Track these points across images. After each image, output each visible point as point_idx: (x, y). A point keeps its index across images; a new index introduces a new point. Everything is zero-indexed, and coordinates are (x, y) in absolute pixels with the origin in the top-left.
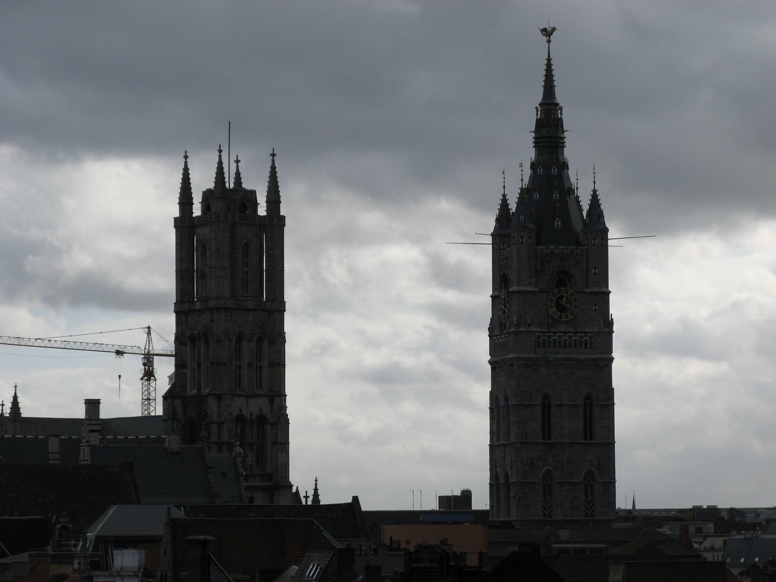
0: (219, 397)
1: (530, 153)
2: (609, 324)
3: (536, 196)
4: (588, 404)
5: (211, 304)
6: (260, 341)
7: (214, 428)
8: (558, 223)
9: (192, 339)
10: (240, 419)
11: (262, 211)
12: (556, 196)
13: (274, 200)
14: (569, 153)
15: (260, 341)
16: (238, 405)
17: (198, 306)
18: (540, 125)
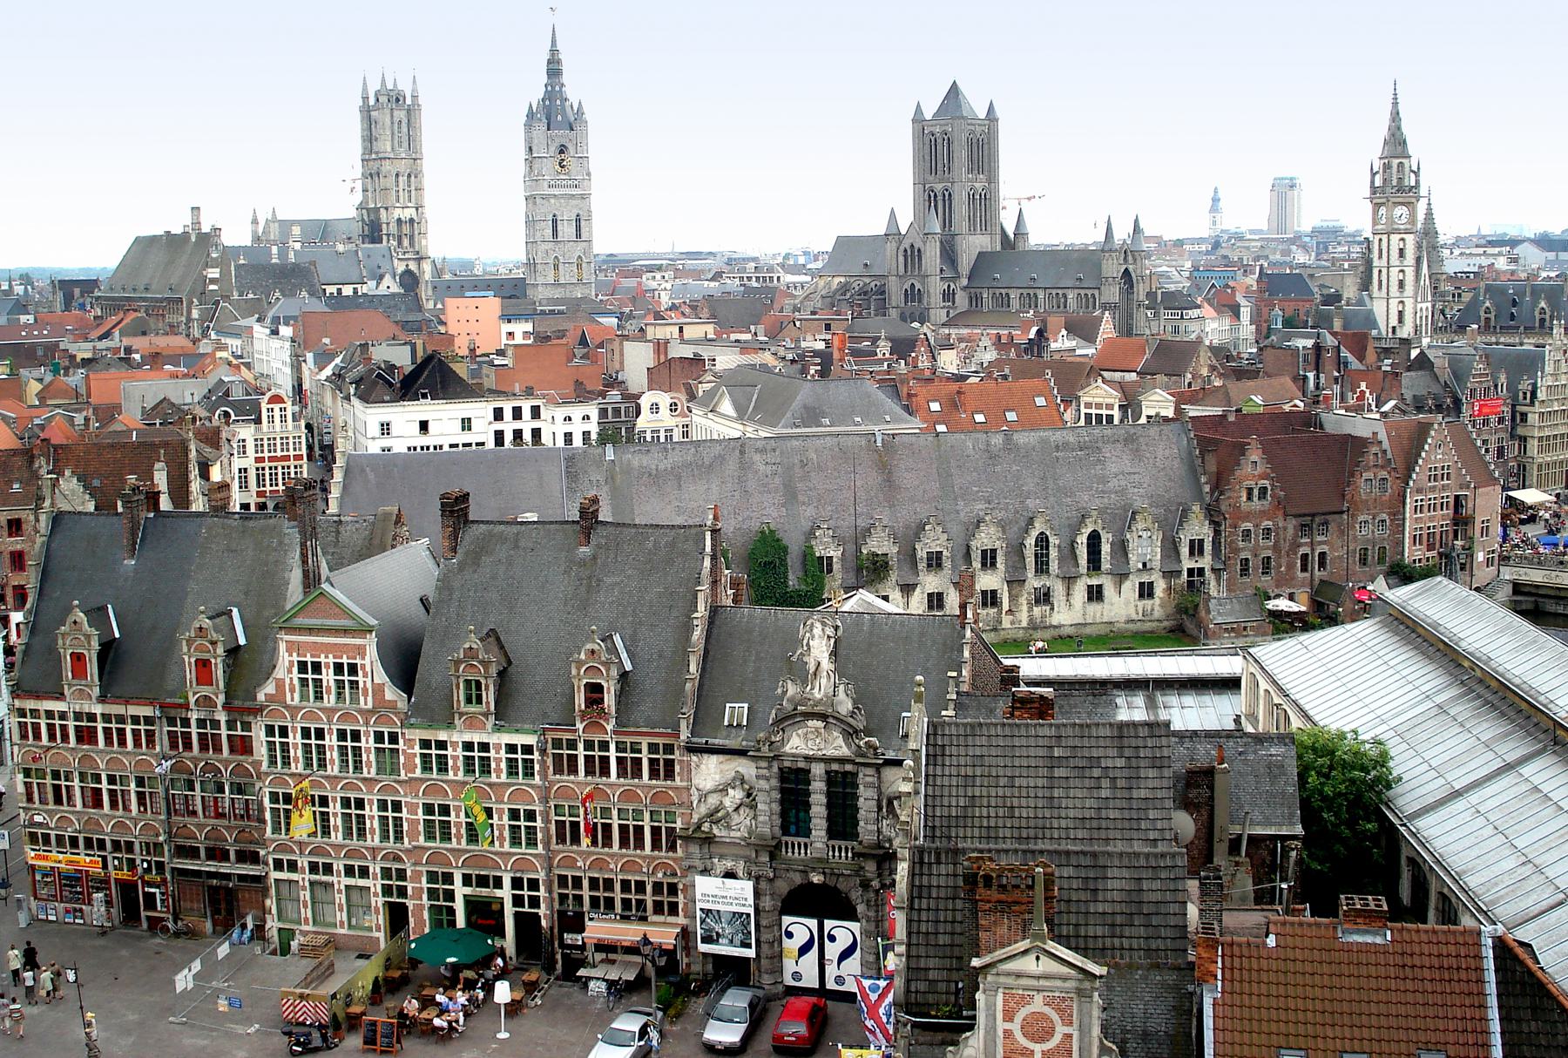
0: (387, 209)
1: (545, 79)
2: (589, 174)
3: (547, 103)
4: (578, 220)
5: (381, 155)
6: (409, 176)
7: (384, 226)
8: (559, 118)
9: (371, 175)
10: (399, 220)
11: (409, 101)
12: (558, 102)
13: (415, 97)
14: (565, 79)
15: (409, 176)
16: (397, 213)
17: (374, 156)
18: (549, 62)
